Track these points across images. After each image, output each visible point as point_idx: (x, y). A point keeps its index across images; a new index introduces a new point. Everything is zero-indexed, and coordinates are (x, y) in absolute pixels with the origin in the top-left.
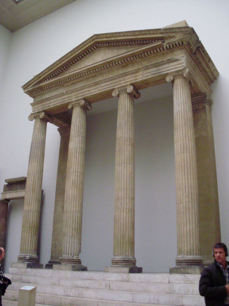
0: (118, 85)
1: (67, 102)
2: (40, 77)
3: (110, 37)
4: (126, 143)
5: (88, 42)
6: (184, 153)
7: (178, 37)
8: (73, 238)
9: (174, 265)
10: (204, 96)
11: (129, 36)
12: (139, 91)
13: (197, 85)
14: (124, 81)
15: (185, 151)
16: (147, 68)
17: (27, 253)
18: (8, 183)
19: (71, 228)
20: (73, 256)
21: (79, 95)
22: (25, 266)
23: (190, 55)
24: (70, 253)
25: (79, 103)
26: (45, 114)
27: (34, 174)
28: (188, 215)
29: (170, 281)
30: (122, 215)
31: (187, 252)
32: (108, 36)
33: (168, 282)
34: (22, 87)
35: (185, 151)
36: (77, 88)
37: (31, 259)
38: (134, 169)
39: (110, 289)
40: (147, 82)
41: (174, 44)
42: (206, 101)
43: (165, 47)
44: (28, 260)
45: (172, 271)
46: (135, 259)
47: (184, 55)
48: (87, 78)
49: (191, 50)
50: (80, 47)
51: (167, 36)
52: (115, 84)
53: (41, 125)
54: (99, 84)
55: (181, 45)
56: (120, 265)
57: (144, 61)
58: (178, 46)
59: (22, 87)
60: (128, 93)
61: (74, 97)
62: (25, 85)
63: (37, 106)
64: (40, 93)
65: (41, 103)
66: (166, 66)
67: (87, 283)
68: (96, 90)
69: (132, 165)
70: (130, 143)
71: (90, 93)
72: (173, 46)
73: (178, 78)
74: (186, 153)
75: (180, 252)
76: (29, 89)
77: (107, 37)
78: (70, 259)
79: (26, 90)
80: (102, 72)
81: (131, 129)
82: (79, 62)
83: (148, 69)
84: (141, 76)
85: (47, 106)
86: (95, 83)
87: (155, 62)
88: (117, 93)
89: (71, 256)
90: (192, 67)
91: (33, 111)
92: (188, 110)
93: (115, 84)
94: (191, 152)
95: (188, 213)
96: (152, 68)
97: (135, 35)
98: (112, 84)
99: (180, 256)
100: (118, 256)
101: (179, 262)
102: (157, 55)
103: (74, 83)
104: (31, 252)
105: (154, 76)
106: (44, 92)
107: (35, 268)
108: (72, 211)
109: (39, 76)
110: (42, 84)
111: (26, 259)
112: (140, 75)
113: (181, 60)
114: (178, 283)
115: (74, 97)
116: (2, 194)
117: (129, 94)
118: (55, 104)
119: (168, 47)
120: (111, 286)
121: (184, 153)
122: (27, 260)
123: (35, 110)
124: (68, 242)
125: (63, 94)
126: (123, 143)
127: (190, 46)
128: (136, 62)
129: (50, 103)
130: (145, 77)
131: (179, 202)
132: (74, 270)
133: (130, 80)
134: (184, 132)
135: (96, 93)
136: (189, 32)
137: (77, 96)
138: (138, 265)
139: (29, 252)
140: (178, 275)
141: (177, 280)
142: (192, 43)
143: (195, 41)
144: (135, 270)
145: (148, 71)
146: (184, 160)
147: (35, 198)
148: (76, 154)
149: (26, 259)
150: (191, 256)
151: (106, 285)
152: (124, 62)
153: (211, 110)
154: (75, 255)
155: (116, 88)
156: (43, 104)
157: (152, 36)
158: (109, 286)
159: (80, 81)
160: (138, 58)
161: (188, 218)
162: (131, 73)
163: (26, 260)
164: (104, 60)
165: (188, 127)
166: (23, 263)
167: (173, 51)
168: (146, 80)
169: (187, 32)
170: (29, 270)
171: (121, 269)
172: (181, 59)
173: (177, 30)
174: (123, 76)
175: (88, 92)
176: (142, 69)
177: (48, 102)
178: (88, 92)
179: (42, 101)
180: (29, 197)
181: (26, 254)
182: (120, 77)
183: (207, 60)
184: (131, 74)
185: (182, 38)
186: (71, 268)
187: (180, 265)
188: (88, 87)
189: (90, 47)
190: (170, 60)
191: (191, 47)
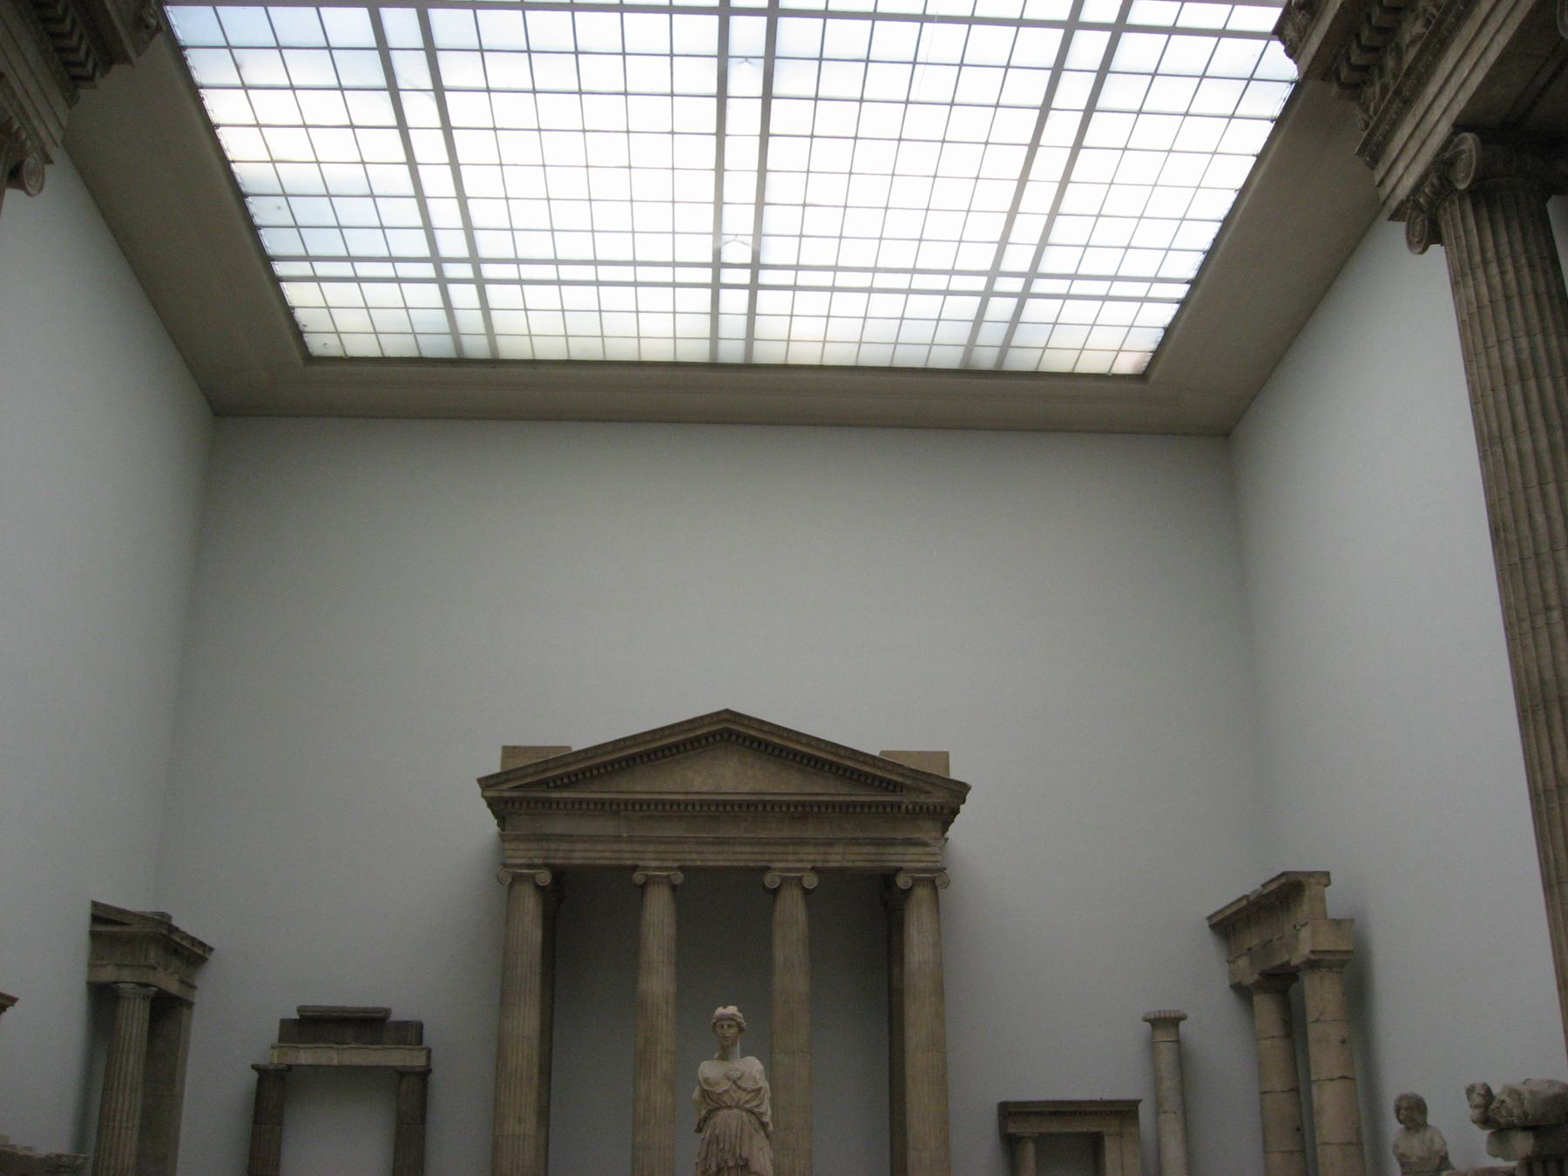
1: (629, 862)
3: (771, 733)
16: (855, 842)
34: (480, 781)
59: (480, 781)
60: (807, 892)
62: (492, 777)
66: (899, 849)
76: (506, 794)
79: (490, 794)
87: (878, 835)
105: (869, 864)
110: (555, 795)
116: (273, 1047)
125: (618, 839)
145: (856, 849)
152: (800, 811)
173: (938, 782)
175: (694, 856)
177: (564, 846)
178: (694, 856)
182: (785, 844)
184: (816, 844)
189: (706, 736)
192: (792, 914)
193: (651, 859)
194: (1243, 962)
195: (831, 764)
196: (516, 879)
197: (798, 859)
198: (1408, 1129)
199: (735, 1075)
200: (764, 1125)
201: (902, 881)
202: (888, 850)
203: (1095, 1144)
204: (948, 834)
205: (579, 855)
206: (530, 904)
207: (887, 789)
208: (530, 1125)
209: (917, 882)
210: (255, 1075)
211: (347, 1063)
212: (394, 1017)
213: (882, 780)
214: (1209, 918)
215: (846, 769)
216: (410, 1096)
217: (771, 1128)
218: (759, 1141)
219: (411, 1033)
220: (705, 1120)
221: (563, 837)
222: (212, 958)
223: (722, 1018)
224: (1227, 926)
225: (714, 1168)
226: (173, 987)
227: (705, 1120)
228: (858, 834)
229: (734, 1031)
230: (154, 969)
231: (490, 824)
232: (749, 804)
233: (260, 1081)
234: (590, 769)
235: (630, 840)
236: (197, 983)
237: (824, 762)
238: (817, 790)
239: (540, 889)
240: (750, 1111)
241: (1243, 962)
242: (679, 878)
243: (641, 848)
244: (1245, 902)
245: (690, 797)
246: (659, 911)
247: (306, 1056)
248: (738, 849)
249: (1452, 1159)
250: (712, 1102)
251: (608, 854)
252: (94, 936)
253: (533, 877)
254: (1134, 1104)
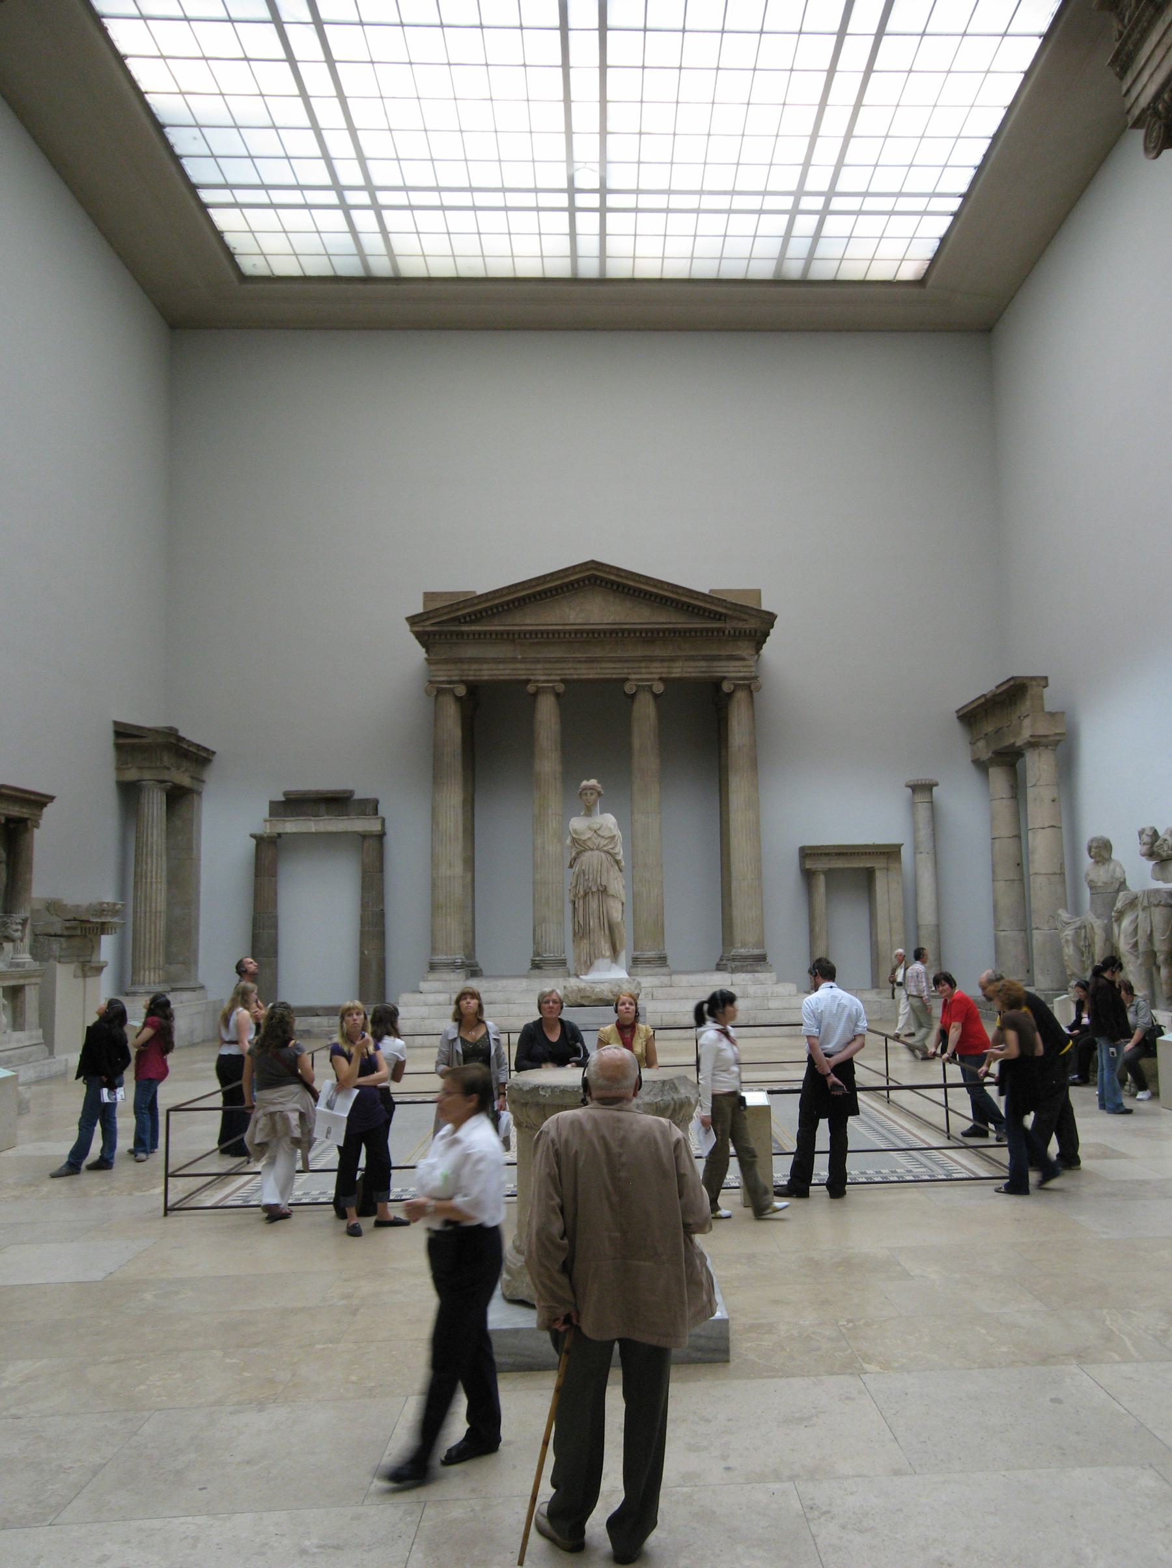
1: (524, 677)
2: (458, 610)
3: (627, 578)
25: (553, 687)
34: (408, 619)
59: (408, 619)
63: (443, 667)
66: (723, 663)
79: (416, 629)
85: (472, 673)
87: (708, 653)
97: (677, 594)
110: (465, 628)
116: (266, 821)
125: (514, 660)
133: (659, 670)
137: (549, 672)
145: (692, 664)
152: (650, 636)
175: (572, 671)
177: (475, 666)
178: (572, 671)
182: (640, 661)
184: (662, 661)
192: (645, 712)
193: (540, 674)
194: (981, 744)
195: (673, 600)
196: (440, 692)
197: (649, 672)
198: (1097, 862)
199: (596, 827)
200: (617, 862)
201: (726, 687)
202: (716, 664)
203: (870, 873)
204: (762, 652)
205: (487, 673)
206: (451, 710)
207: (714, 618)
208: (458, 869)
209: (737, 687)
210: (254, 841)
211: (322, 830)
212: (356, 797)
213: (710, 611)
214: (957, 712)
215: (684, 603)
216: (372, 849)
217: (623, 864)
218: (614, 872)
219: (370, 807)
220: (575, 859)
221: (473, 660)
222: (215, 759)
223: (586, 788)
224: (971, 717)
225: (582, 893)
226: (185, 780)
227: (575, 859)
228: (693, 653)
229: (595, 795)
230: (168, 769)
231: (421, 652)
232: (612, 632)
233: (257, 845)
234: (491, 608)
235: (523, 661)
236: (205, 777)
237: (667, 598)
238: (662, 620)
239: (458, 699)
240: (607, 852)
241: (981, 744)
242: (561, 688)
243: (533, 666)
244: (983, 700)
245: (568, 627)
246: (547, 712)
247: (291, 826)
249: (1128, 883)
250: (580, 847)
251: (507, 672)
252: (118, 747)
253: (452, 691)
254: (899, 846)
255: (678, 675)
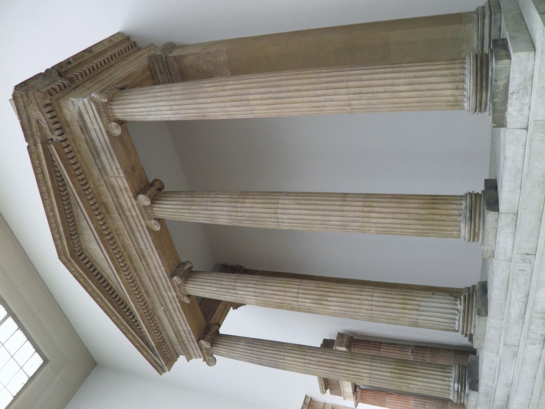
0: (140, 221)
1: (179, 305)
3: (59, 232)
4: (239, 209)
5: (73, 269)
6: (248, 100)
7: (36, 114)
8: (421, 308)
9: (487, 117)
10: (153, 59)
11: (51, 201)
12: (150, 181)
13: (131, 74)
14: (132, 210)
15: (245, 97)
16: (102, 170)
17: (449, 386)
18: (326, 389)
19: (402, 311)
20: (458, 310)
21: (165, 284)
22: (473, 394)
23: (75, 88)
24: (451, 316)
25: (179, 286)
26: (203, 339)
27: (304, 363)
28: (375, 89)
29: (524, 125)
30: (375, 220)
31: (457, 89)
32: (58, 236)
33: (524, 132)
35: (245, 97)
36: (154, 288)
37: (461, 380)
38: (288, 194)
39: (534, 253)
40: (130, 170)
41: (51, 121)
42: (164, 56)
43: (60, 138)
44: (463, 386)
45: (500, 122)
46: (466, 195)
47: (70, 102)
48: (135, 270)
49: (63, 87)
50: (84, 283)
51: (38, 134)
52: (139, 224)
53: (221, 346)
54: (142, 252)
55: (52, 109)
56: (479, 228)
57: (93, 174)
58: (54, 114)
60: (152, 203)
61: (170, 294)
64: (170, 345)
65: (185, 345)
67: (517, 296)
68: (153, 256)
69: (279, 199)
70: (240, 200)
71: (160, 267)
72: (56, 123)
73: (112, 112)
74: (248, 94)
75: (457, 104)
76: (164, 363)
77: (60, 238)
78: (464, 317)
80: (120, 245)
81: (215, 199)
82: (111, 283)
83: (104, 167)
84: (119, 179)
85: (188, 336)
86: (140, 259)
88: (153, 221)
89: (457, 315)
90: (95, 84)
91: (201, 357)
92: (168, 93)
93: (139, 224)
94: (247, 86)
95: (370, 90)
96: (101, 161)
98: (139, 231)
99: (466, 105)
100: (460, 231)
101: (479, 107)
102: (79, 151)
103: (147, 292)
104: (447, 379)
105: (115, 157)
106: (167, 339)
107: (477, 374)
108: (369, 307)
109: (139, 347)
111: (460, 390)
112: (118, 182)
113: (79, 108)
114: (530, 108)
115: (170, 294)
117: (154, 200)
118: (185, 323)
119: (59, 132)
120: (526, 251)
121: (248, 100)
122: (463, 389)
123: (197, 355)
124: (430, 318)
126: (240, 214)
127: (53, 89)
128: (96, 189)
129: (184, 331)
130: (119, 174)
131: (349, 108)
132: (487, 313)
133: (128, 199)
134: (209, 100)
135: (158, 257)
136: (24, 94)
138: (479, 188)
139: (447, 383)
140: (510, 110)
141: (521, 110)
142: (48, 85)
143: (46, 80)
144: (489, 197)
145: (108, 168)
146: (262, 99)
147: (348, 364)
148: (265, 295)
149: (460, 390)
150: (467, 79)
151: (524, 261)
153: (183, 46)
154: (454, 307)
155: (146, 224)
156: (186, 342)
157: (44, 161)
158: (528, 254)
159: (141, 281)
160: (87, 186)
161: (382, 89)
162: (115, 198)
163: (461, 390)
164: (99, 244)
165: (200, 93)
166: (467, 396)
167: (67, 122)
168: (125, 172)
169: (25, 98)
170: (482, 387)
171: (488, 226)
172: (77, 107)
173: (24, 117)
174: (124, 212)
175: (159, 271)
176: (106, 178)
177: (183, 333)
178: (159, 271)
179: (182, 343)
180: (345, 375)
181: (452, 389)
182: (127, 218)
183: (87, 55)
184: (117, 197)
185: (38, 106)
186: (483, 318)
187: (486, 105)
188: (150, 270)
190: (81, 129)
191: (57, 87)
222: (310, 395)
236: (323, 402)
248: (143, 246)
251: (179, 315)
255: (125, 181)
